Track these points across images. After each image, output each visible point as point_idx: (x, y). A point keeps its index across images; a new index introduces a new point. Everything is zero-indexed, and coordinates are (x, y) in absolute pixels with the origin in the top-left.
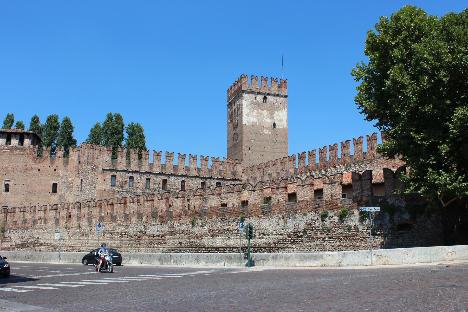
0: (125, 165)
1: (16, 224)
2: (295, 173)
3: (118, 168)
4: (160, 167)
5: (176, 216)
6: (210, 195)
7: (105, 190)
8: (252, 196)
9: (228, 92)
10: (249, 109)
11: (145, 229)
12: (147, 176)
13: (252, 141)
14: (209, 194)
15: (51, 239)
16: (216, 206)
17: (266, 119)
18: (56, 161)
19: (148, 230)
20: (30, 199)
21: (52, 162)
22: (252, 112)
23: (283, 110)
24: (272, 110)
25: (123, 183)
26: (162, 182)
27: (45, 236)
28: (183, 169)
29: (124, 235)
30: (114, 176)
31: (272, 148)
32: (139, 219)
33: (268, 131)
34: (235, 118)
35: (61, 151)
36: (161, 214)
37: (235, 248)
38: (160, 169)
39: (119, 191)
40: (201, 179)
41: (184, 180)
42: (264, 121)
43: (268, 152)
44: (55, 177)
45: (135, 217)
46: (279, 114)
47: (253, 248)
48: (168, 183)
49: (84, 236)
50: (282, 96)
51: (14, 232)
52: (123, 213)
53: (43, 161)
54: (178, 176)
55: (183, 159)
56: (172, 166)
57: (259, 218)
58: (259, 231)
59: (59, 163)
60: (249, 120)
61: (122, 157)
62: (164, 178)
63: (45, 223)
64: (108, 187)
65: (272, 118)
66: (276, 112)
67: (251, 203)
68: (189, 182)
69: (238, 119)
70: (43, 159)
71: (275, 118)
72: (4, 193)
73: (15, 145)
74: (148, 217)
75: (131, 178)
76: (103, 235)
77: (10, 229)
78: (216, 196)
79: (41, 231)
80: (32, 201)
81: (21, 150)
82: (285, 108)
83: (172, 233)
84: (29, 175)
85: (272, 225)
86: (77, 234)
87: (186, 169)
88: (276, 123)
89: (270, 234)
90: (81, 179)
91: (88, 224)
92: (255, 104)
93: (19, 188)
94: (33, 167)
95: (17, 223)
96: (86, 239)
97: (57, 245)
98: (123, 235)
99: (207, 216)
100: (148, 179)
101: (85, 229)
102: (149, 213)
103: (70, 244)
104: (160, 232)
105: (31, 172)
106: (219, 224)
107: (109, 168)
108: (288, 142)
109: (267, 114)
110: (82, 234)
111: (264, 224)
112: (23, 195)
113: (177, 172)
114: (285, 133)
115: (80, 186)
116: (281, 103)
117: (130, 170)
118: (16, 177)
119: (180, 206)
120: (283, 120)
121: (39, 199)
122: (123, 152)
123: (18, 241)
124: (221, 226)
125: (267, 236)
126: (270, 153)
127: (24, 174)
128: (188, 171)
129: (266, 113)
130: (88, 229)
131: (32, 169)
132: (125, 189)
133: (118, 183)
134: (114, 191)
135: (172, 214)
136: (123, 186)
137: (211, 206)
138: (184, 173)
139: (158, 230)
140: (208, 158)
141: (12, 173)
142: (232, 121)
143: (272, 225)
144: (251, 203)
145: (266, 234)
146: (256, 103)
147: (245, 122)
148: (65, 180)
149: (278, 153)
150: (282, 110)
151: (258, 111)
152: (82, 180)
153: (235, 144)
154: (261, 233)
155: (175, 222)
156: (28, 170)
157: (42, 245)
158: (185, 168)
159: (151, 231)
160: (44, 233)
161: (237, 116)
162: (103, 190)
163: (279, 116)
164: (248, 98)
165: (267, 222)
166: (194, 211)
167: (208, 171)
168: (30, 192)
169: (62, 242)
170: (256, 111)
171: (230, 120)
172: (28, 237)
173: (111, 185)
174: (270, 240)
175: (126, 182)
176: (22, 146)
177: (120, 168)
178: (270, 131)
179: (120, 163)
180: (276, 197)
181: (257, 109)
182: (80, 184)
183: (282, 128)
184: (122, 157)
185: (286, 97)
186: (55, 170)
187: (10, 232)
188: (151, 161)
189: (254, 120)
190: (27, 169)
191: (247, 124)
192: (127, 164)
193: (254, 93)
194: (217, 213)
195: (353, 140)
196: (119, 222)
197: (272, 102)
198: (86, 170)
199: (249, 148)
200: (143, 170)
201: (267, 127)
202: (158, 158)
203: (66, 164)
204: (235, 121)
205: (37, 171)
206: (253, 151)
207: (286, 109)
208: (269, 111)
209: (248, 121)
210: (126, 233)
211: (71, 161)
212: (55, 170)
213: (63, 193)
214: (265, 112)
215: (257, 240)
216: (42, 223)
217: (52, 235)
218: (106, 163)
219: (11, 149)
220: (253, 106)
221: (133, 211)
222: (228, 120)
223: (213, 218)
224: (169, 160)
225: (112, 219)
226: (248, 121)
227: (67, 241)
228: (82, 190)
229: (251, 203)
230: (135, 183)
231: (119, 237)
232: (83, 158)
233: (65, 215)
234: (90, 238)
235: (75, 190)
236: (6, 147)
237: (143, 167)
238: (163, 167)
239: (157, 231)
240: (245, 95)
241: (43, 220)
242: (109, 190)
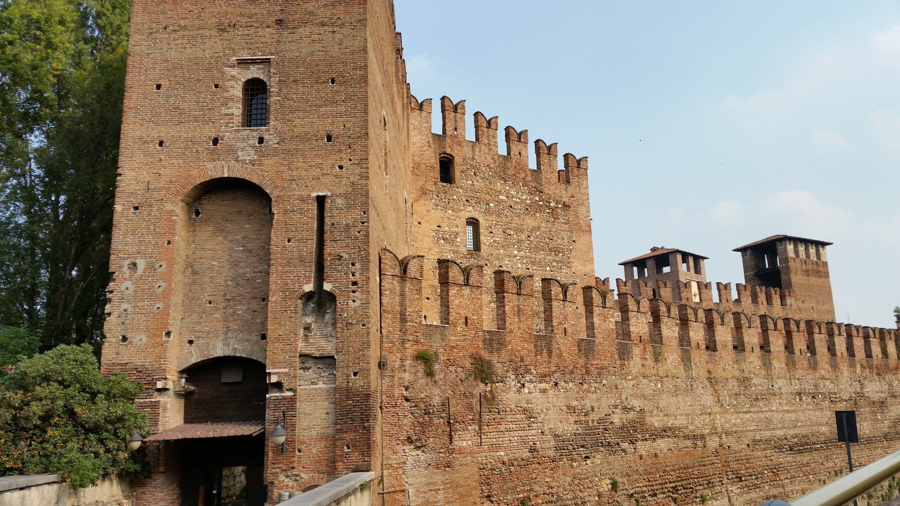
1: (550, 352)
76: (800, 400)
95: (555, 345)
96: (765, 409)
169: (707, 421)
196: (823, 372)
227: (718, 416)
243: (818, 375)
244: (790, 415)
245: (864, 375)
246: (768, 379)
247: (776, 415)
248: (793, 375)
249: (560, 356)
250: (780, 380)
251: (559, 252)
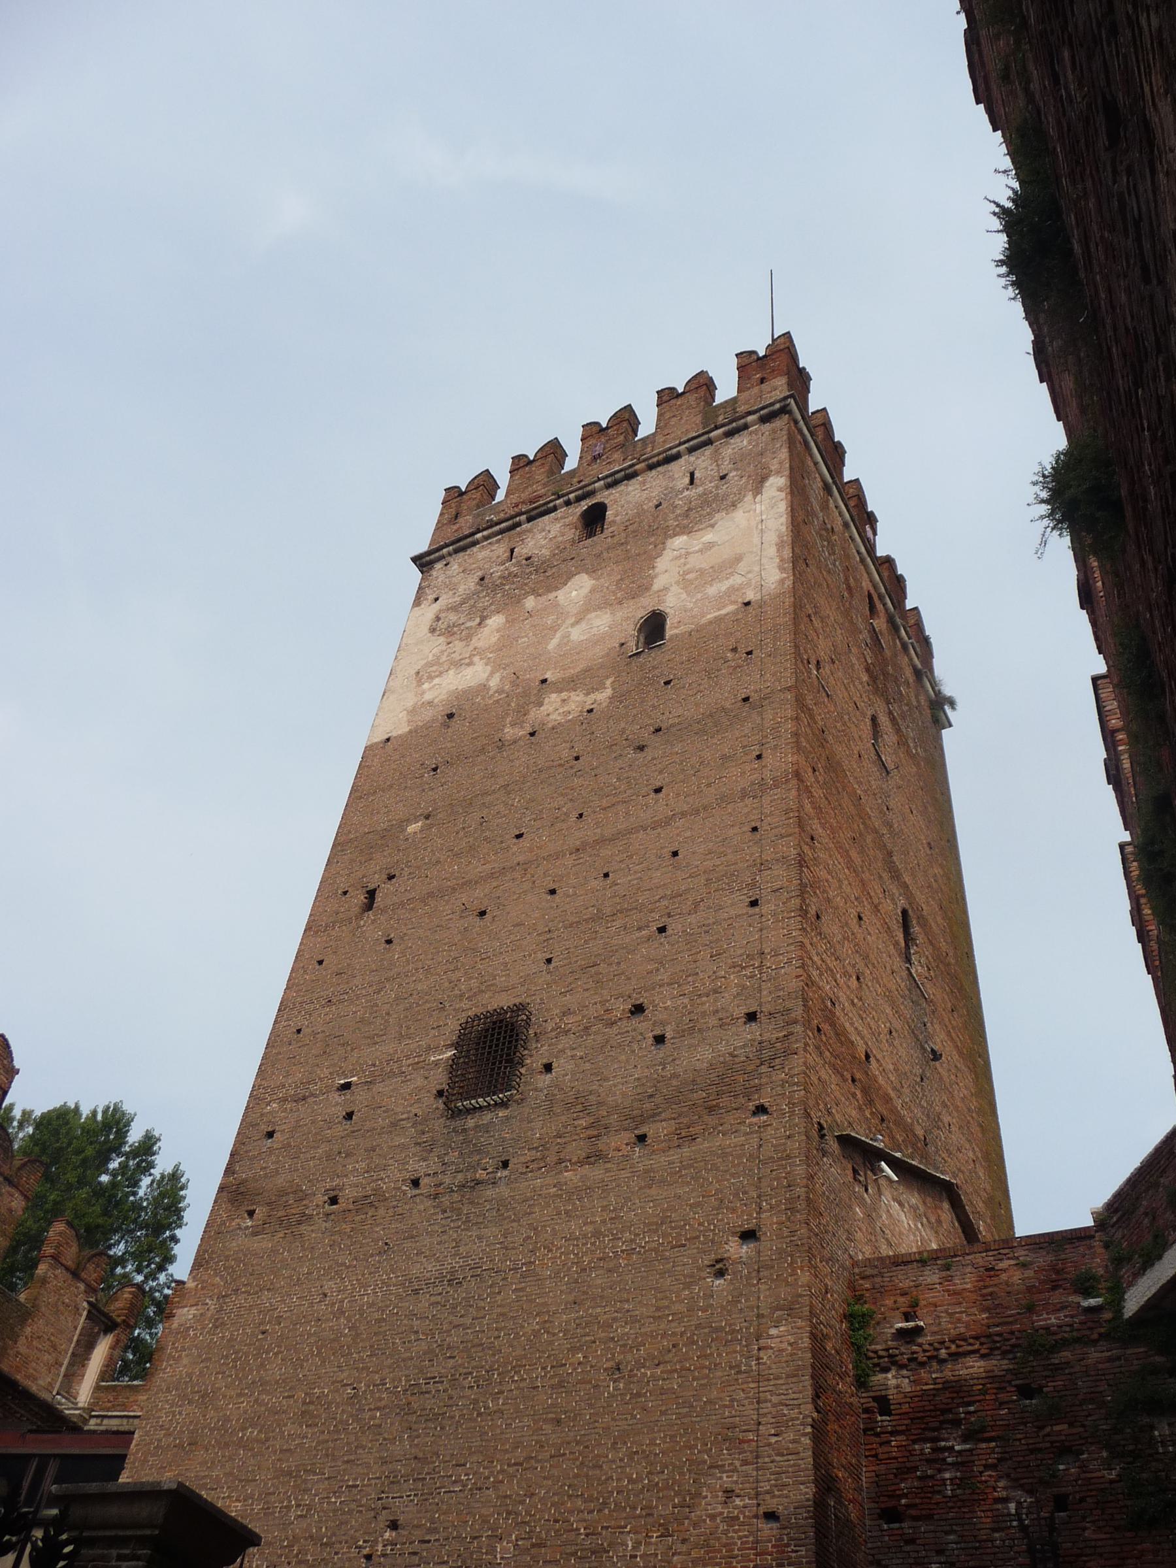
10: (450, 632)
13: (412, 828)
23: (749, 497)
31: (604, 803)
42: (552, 644)
43: (558, 856)
46: (709, 537)
60: (428, 697)
66: (679, 541)
82: (764, 479)
109: (592, 591)
126: (569, 860)
129: (585, 591)
149: (668, 821)
150: (734, 505)
178: (601, 687)
183: (731, 608)
199: (371, 894)
201: (578, 669)
207: (776, 485)
220: (486, 601)
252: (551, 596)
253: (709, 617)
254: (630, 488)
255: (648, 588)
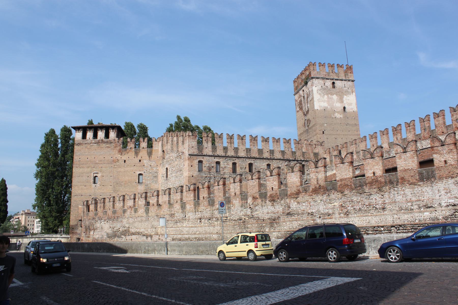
0: (211, 150)
1: (106, 215)
2: (390, 148)
3: (205, 153)
4: (245, 151)
5: (292, 194)
6: (338, 165)
7: (193, 176)
8: (401, 160)
9: (295, 82)
10: (320, 94)
11: (251, 213)
12: (234, 161)
13: (325, 125)
14: (338, 163)
15: (142, 228)
16: (348, 177)
17: (336, 103)
18: (141, 152)
19: (256, 213)
20: (117, 190)
21: (137, 154)
22: (323, 97)
24: (341, 94)
25: (210, 169)
26: (248, 166)
27: (136, 225)
28: (268, 152)
29: (225, 219)
30: (200, 162)
32: (243, 201)
33: (339, 115)
34: (305, 106)
35: (145, 142)
36: (271, 193)
37: (382, 227)
38: (246, 153)
39: (206, 177)
40: (286, 162)
41: (269, 163)
42: (334, 105)
43: (342, 135)
44: (140, 167)
45: (238, 199)
46: (348, 98)
47: (410, 226)
48: (254, 167)
49: (178, 224)
50: (349, 81)
51: (105, 222)
52: (222, 196)
53: (128, 153)
54: (263, 159)
55: (267, 142)
56: (257, 150)
57: (416, 187)
58: (418, 203)
59: (143, 153)
60: (321, 105)
61: (207, 142)
62: (250, 162)
63: (135, 212)
64: (196, 173)
65: (342, 102)
66: (345, 96)
67: (403, 168)
68: (274, 165)
69: (309, 105)
70: (128, 151)
71: (345, 102)
72: (94, 185)
73: (101, 139)
74: (254, 198)
75: (218, 163)
76: (200, 222)
77: (100, 219)
78: (347, 165)
79: (131, 220)
80: (119, 192)
81: (107, 142)
82: (353, 92)
83: (288, 214)
84: (115, 166)
85: (438, 193)
86: (170, 221)
87: (270, 152)
88: (346, 106)
89: (436, 205)
90: (166, 167)
91: (181, 211)
92: (324, 89)
93: (107, 180)
94: (119, 158)
95: (107, 213)
96: (180, 226)
97: (148, 234)
98: (224, 220)
99: (336, 190)
100: (234, 164)
101: (179, 215)
102: (256, 193)
103: (163, 232)
104: (272, 214)
105: (117, 164)
106: (355, 198)
107: (196, 154)
108: (359, 125)
109: (337, 99)
110: (175, 221)
111: (425, 193)
112: (111, 187)
113: (262, 155)
114: (355, 116)
115: (165, 175)
116: (349, 87)
117: (216, 154)
118: (103, 169)
119: (297, 182)
120: (352, 104)
121: (126, 190)
122: (209, 137)
123: (110, 231)
124: (358, 201)
125: (431, 209)
126: (343, 136)
127: (111, 166)
128: (272, 154)
130: (182, 215)
131: (119, 160)
132: (212, 175)
133: (204, 169)
134: (202, 177)
135: (287, 192)
136: (210, 171)
137: (342, 178)
138: (269, 156)
139: (269, 211)
140: (291, 141)
141: (101, 165)
142: (301, 109)
143: (438, 193)
144: (402, 168)
145: (429, 205)
146: (325, 88)
147: (316, 107)
148: (149, 170)
150: (350, 94)
151: (328, 96)
152: (167, 169)
153: (307, 130)
154: (421, 205)
155: (292, 201)
156: (115, 162)
157: (133, 234)
158: (269, 152)
159: (259, 214)
160: (134, 222)
161: (308, 103)
162: (190, 176)
163: (349, 100)
164: (318, 84)
165: (430, 191)
166: (318, 186)
167: (291, 153)
168: (117, 184)
169: (154, 230)
170: (326, 96)
171: (299, 107)
172: (118, 227)
173: (199, 171)
174: (437, 213)
175: (213, 167)
176: (108, 140)
177: (206, 153)
179: (206, 148)
180: (441, 157)
181: (327, 94)
182: (165, 173)
183: (352, 111)
184: (207, 142)
185: (353, 81)
186: (140, 161)
187: (101, 222)
188: (236, 145)
189: (325, 105)
190: (113, 161)
191: (319, 109)
192: (212, 149)
193: (323, 79)
194: (351, 185)
195: (449, 109)
197: (341, 87)
198: (171, 158)
200: (229, 154)
201: (338, 111)
202: (242, 141)
203: (150, 154)
204: (305, 108)
205: (123, 163)
206: (327, 135)
208: (338, 96)
209: (319, 106)
210: (227, 218)
211: (154, 151)
212: (140, 161)
213: (148, 182)
214: (335, 97)
215: (416, 215)
216: (132, 212)
217: (143, 223)
218: (192, 148)
219: (98, 143)
220: (323, 92)
221: (235, 193)
222: (296, 108)
223: (346, 192)
224: (253, 144)
225: (209, 203)
226: (320, 106)
228: (168, 178)
229: (403, 168)
230: (222, 167)
231: (219, 222)
232: (166, 147)
233: (155, 202)
234: (184, 226)
235: (161, 179)
236: (93, 141)
237: (228, 152)
238: (248, 150)
239: (268, 213)
240: (315, 81)
241: (133, 209)
242: (197, 176)
243: (214, 208)
244: (193, 228)
245: (256, 203)
246: (183, 213)
247: (185, 228)
248: (197, 210)
249: (108, 215)
250: (190, 213)
251: (181, 171)
252: (332, 96)
253: (350, 111)
254: (338, 82)
255: (343, 102)
